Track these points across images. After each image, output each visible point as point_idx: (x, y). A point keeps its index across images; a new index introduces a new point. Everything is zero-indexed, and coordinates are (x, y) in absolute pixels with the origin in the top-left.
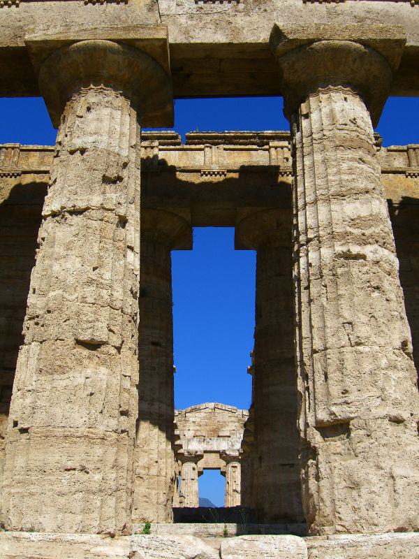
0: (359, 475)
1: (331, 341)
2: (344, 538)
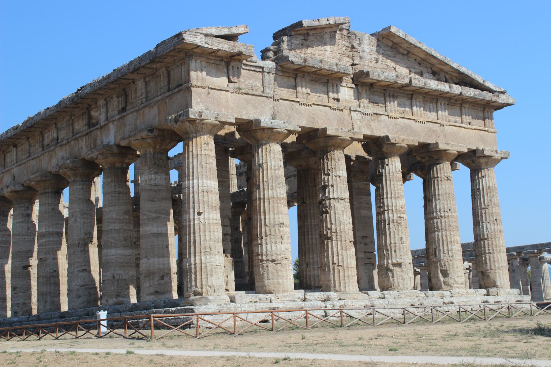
0: (405, 277)
1: (397, 242)
2: (403, 291)
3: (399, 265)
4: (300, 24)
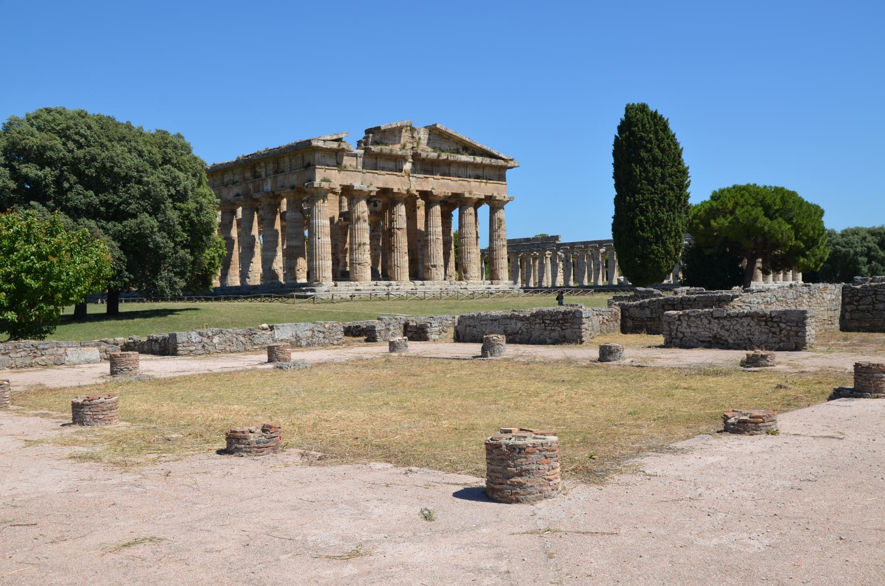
3: (435, 266)
4: (379, 128)
